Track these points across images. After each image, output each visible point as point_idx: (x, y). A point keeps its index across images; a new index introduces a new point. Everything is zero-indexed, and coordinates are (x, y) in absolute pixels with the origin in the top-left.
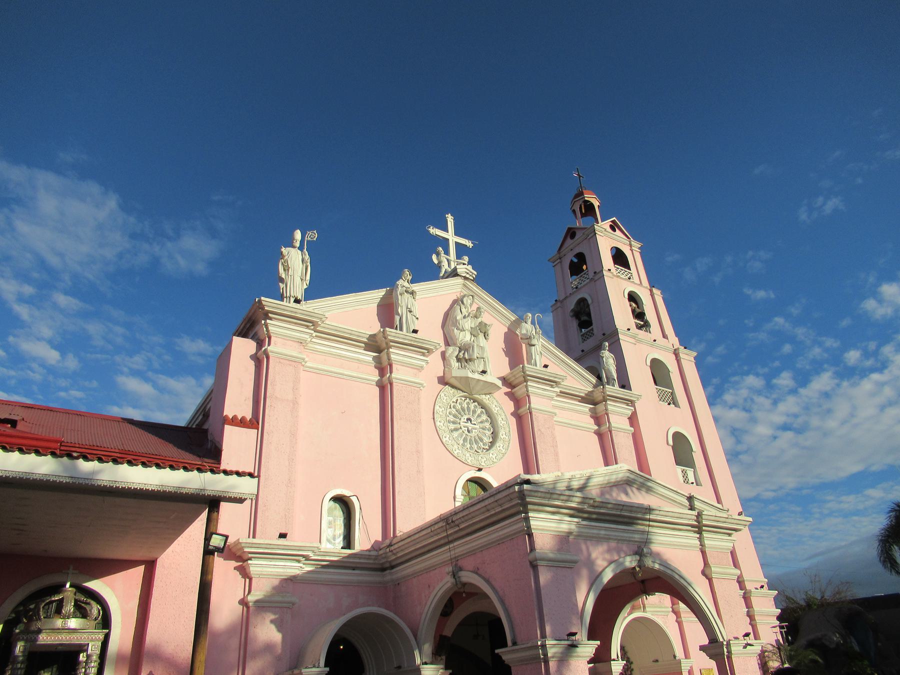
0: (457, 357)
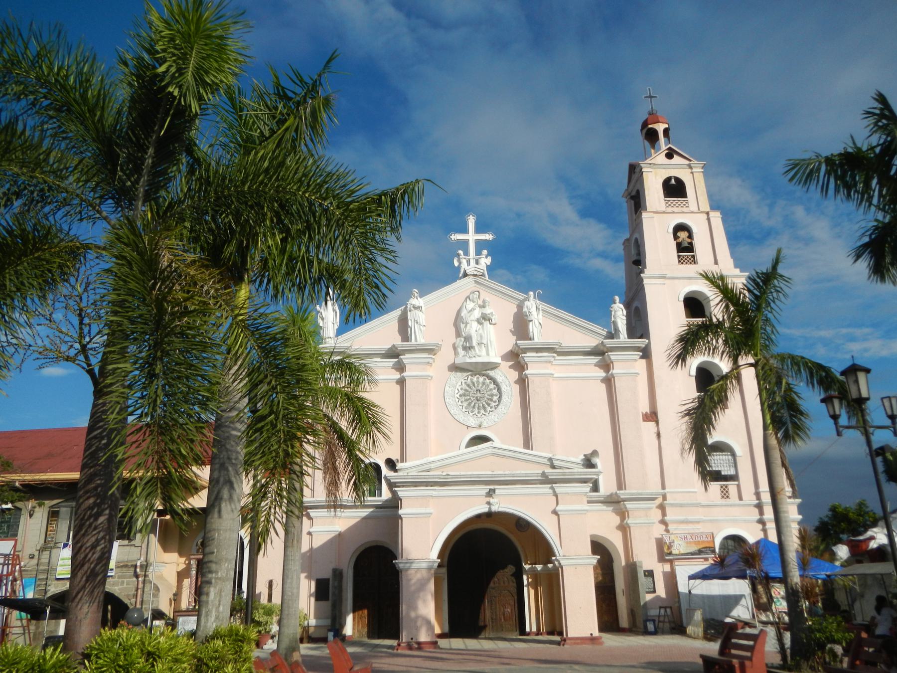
0: (463, 346)
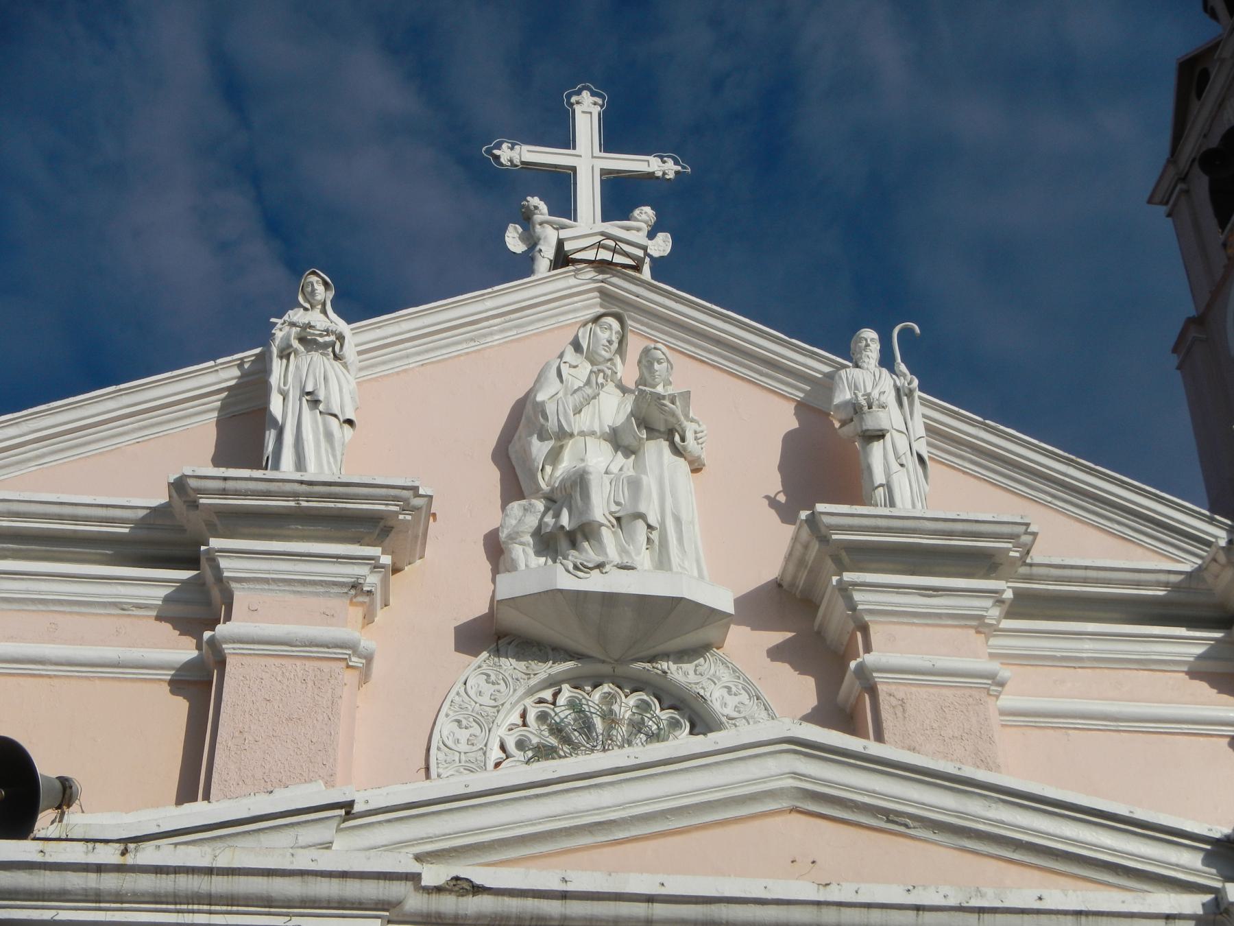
0: (538, 533)
